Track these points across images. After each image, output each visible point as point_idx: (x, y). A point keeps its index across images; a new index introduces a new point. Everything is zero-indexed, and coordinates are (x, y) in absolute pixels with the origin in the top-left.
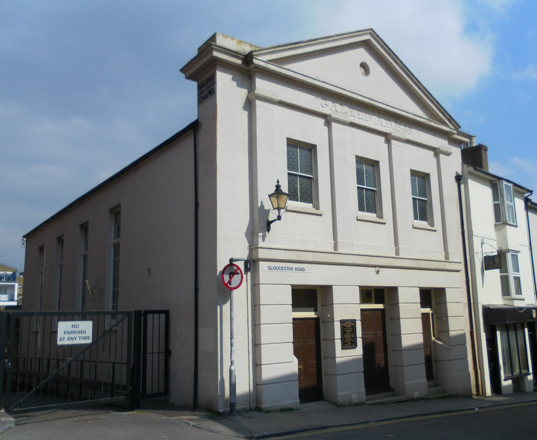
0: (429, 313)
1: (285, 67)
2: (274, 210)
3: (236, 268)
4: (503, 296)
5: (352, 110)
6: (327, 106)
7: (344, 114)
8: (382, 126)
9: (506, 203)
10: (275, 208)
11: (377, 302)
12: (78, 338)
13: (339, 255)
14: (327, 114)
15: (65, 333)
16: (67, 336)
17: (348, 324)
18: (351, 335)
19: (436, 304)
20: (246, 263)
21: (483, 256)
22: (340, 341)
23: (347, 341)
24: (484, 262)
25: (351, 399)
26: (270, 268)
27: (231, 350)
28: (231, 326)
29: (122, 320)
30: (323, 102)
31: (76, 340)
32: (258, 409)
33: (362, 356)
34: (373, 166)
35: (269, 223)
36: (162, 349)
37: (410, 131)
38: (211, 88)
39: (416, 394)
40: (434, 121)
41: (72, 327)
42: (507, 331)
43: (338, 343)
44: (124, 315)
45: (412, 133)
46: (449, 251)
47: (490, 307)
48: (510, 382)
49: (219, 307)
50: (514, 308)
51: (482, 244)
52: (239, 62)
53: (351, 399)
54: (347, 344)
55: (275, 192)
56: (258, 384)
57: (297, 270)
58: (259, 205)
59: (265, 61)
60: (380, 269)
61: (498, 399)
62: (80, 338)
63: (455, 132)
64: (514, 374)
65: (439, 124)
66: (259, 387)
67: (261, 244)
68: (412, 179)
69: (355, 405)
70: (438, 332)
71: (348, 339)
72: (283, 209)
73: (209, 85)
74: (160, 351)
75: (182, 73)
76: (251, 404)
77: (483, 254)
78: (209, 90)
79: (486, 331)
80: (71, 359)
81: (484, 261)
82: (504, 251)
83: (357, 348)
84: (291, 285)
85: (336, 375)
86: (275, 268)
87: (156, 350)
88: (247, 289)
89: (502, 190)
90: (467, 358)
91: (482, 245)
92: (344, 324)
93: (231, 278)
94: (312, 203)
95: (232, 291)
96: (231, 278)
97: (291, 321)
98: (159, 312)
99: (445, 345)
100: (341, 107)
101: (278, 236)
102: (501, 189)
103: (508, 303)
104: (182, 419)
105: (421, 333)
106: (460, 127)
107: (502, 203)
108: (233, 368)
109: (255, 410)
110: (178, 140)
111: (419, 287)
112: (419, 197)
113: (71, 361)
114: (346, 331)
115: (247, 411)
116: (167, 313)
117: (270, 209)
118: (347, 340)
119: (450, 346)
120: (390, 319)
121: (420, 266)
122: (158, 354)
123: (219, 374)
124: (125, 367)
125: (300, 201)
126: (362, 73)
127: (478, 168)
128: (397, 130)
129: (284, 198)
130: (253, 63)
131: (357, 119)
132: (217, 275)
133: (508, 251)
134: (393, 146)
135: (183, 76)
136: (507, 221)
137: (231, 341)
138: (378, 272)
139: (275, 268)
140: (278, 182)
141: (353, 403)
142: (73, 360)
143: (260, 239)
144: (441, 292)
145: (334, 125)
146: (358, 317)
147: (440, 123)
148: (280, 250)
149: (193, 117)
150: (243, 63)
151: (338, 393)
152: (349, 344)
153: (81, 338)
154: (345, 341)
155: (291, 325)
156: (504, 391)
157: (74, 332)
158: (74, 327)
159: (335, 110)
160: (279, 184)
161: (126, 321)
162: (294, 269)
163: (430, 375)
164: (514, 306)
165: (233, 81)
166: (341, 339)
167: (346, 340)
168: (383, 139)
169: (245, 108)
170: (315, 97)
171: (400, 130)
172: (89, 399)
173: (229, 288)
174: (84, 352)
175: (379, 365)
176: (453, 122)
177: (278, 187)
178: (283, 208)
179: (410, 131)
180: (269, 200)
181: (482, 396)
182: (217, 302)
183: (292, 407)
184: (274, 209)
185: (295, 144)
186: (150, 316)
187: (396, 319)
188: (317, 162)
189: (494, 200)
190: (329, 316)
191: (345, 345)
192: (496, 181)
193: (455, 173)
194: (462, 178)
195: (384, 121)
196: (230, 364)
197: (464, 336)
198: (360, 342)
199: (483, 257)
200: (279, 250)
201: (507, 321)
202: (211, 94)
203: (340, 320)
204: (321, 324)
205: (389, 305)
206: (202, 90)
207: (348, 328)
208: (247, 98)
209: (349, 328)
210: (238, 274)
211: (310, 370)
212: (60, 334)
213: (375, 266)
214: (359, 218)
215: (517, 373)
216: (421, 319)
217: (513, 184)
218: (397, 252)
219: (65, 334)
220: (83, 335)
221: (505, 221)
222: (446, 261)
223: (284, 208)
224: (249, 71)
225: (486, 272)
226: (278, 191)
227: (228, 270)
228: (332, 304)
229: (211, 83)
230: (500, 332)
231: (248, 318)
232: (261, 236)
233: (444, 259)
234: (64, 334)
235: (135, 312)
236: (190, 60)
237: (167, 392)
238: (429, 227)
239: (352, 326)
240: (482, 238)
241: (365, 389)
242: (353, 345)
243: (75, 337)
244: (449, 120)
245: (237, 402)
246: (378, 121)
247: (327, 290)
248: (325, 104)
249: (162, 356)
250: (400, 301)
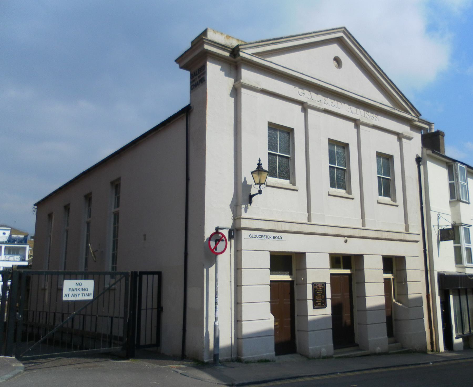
0: (391, 278)
1: (267, 59)
2: (255, 185)
3: (221, 236)
4: (456, 264)
5: (326, 98)
6: (304, 94)
7: (319, 102)
8: (352, 113)
9: (460, 183)
10: (256, 183)
11: (345, 268)
12: (81, 295)
13: (312, 225)
14: (304, 102)
15: (69, 290)
16: (71, 293)
17: (319, 287)
18: (321, 296)
19: (397, 270)
20: (230, 231)
21: (439, 228)
22: (312, 301)
23: (318, 301)
24: (440, 234)
25: (320, 352)
26: (251, 236)
27: (216, 308)
28: (216, 287)
29: (120, 280)
30: (301, 91)
31: (79, 296)
32: (239, 360)
33: (330, 315)
34: (344, 148)
35: (251, 197)
36: (155, 306)
37: (376, 117)
38: (202, 77)
39: (378, 349)
40: (398, 109)
41: (76, 285)
42: (459, 295)
43: (310, 303)
44: (122, 276)
45: (378, 119)
46: (409, 224)
47: (444, 274)
48: (460, 340)
49: (205, 270)
50: (466, 275)
51: (438, 218)
52: (227, 54)
53: (320, 352)
54: (318, 304)
55: (257, 169)
56: (239, 338)
57: (275, 238)
58: (243, 180)
59: (250, 53)
60: (348, 239)
61: (450, 354)
62: (83, 295)
63: (416, 119)
64: (465, 333)
65: (402, 112)
66: (240, 340)
67: (244, 215)
68: (377, 160)
69: (324, 358)
70: (398, 295)
71: (319, 300)
72: (264, 185)
73: (200, 74)
74: (153, 308)
75: (177, 63)
76: (232, 355)
77: (439, 227)
78: (200, 78)
79: (440, 294)
80: (74, 313)
81: (439, 233)
82: (458, 225)
83: (326, 308)
84: (269, 251)
85: (308, 331)
86: (256, 236)
87: (149, 306)
88: (231, 254)
89: (456, 171)
90: (423, 318)
91: (438, 219)
92: (316, 287)
93: (216, 244)
94: (289, 180)
95: (217, 256)
96: (216, 244)
97: (269, 283)
98: (153, 273)
99: (404, 306)
100: (316, 95)
101: (259, 208)
102: (456, 170)
103: (461, 270)
104: (171, 367)
105: (383, 295)
106: (420, 115)
107: (457, 182)
108: (217, 323)
109: (236, 361)
110: (172, 122)
111: (382, 255)
112: (383, 176)
113: (74, 315)
114: (317, 293)
115: (229, 361)
116: (159, 274)
117: (252, 184)
118: (318, 301)
119: (408, 307)
120: (356, 283)
121: (383, 237)
122: (151, 310)
123: (205, 329)
124: (122, 321)
125: (279, 178)
126: (335, 66)
127: (436, 151)
128: (365, 117)
129: (265, 174)
131: (330, 106)
132: (204, 241)
133: (461, 225)
134: (361, 131)
135: (178, 65)
136: (460, 199)
137: (216, 300)
138: (346, 241)
139: (256, 236)
140: (259, 160)
141: (323, 356)
142: (76, 314)
143: (243, 210)
144: (401, 259)
145: (310, 111)
146: (327, 280)
148: (261, 221)
149: (185, 102)
150: (230, 55)
151: (309, 347)
152: (319, 304)
153: (84, 295)
154: (316, 301)
155: (269, 287)
156: (455, 348)
157: (77, 290)
158: (78, 285)
159: (311, 98)
160: (261, 162)
161: (123, 280)
162: (272, 237)
163: (390, 333)
164: (465, 273)
165: (221, 71)
166: (313, 300)
167: (317, 301)
168: (352, 124)
169: (231, 95)
170: (293, 86)
171: (368, 117)
172: (90, 349)
173: (215, 253)
174: (86, 307)
175: (346, 323)
176: (414, 110)
177: (259, 165)
178: (263, 184)
180: (252, 175)
181: (436, 352)
182: (204, 266)
183: (268, 358)
184: (256, 184)
185: (275, 128)
186: (144, 277)
187: (362, 283)
188: (294, 143)
189: (450, 180)
190: (302, 279)
191: (316, 305)
192: (452, 163)
193: (416, 155)
194: (422, 159)
195: (353, 109)
196: (215, 320)
197: (420, 299)
198: (329, 302)
199: (439, 230)
200: (260, 221)
201: (459, 287)
202: (202, 82)
203: (312, 283)
204: (295, 287)
205: (356, 270)
206: (194, 79)
207: (319, 290)
208: (234, 86)
209: (320, 290)
210: (223, 241)
211: (285, 326)
212: (65, 291)
213: (344, 236)
214: (330, 194)
215: (467, 332)
216: (383, 284)
217: (466, 166)
218: (363, 224)
219: (70, 291)
220: (85, 292)
221: (459, 198)
222: (406, 232)
223: (264, 184)
224: (236, 62)
225: (441, 243)
226: (259, 169)
227: (214, 238)
228: (305, 269)
229: (202, 73)
230: (453, 296)
231: (231, 280)
232: (244, 208)
233: (404, 231)
234: (69, 291)
235: (132, 272)
236: (184, 52)
237: (158, 343)
238: (392, 203)
239: (322, 288)
240: (438, 213)
241: (333, 344)
242: (323, 305)
243: (78, 294)
244: (411, 109)
245: (220, 353)
246: (349, 109)
247: (301, 256)
248: (302, 93)
249: (155, 312)
250: (365, 267)
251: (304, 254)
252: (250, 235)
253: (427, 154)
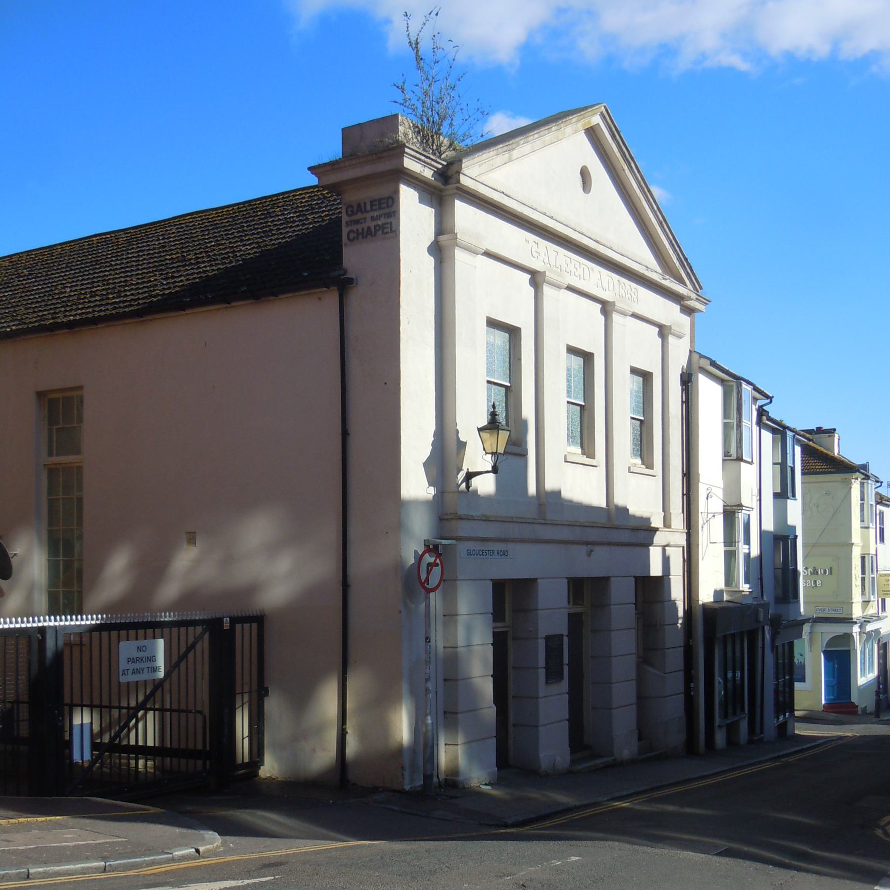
10: (487, 452)
12: (146, 670)
15: (128, 661)
29: (202, 634)
46: (671, 511)
62: (148, 670)
75: (312, 173)
83: (562, 681)
106: (701, 288)
138: (589, 554)
147: (677, 281)
157: (140, 660)
161: (207, 636)
162: (496, 553)
166: (545, 668)
173: (425, 588)
179: (635, 295)
184: (486, 453)
186: (238, 627)
204: (510, 643)
206: (355, 217)
213: (587, 543)
224: (441, 191)
229: (386, 211)
240: (708, 486)
246: (598, 280)
248: (536, 252)
251: (534, 581)
252: (468, 550)
253: (700, 366)
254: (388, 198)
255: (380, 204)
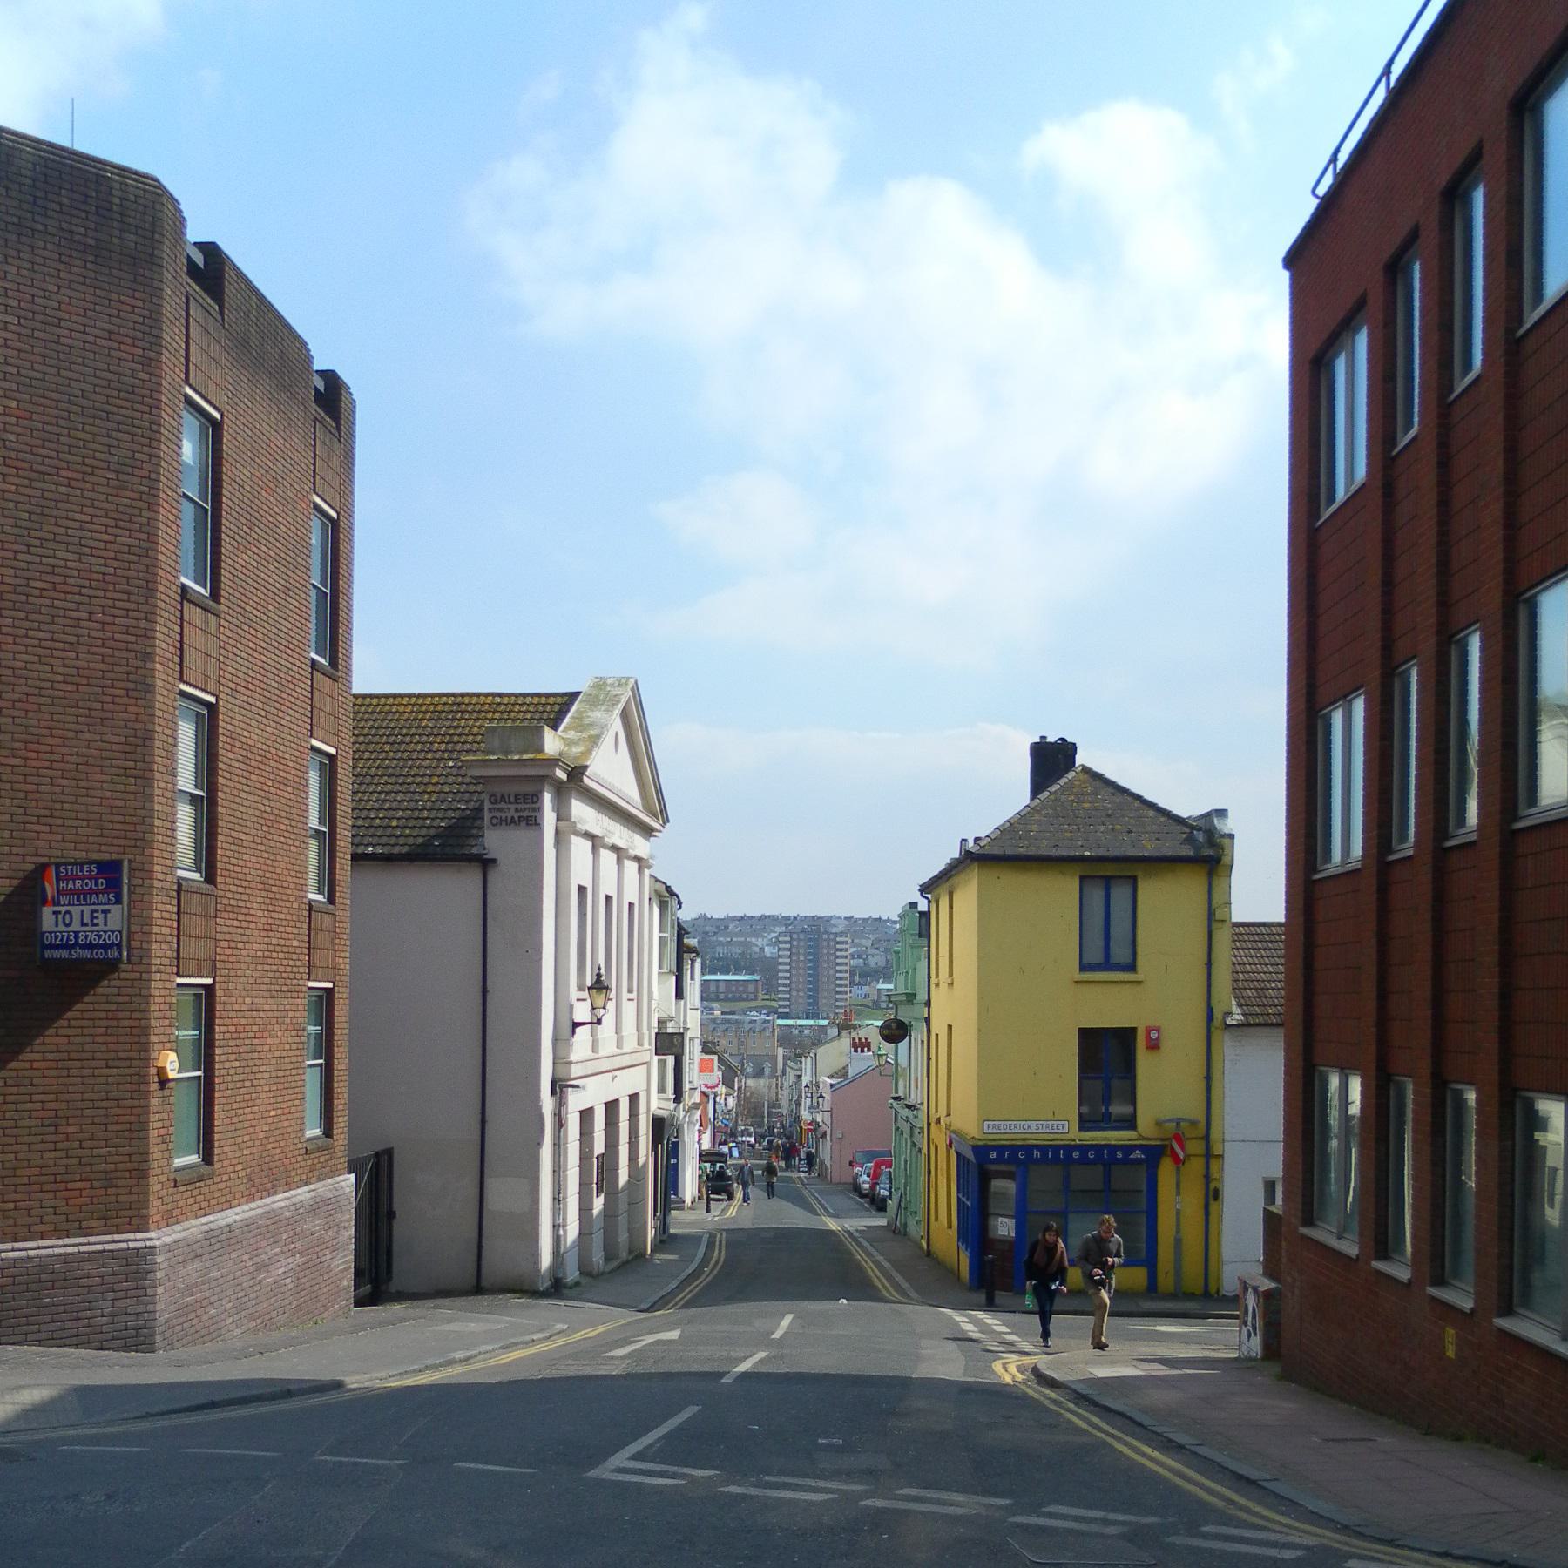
73: (522, 806)
78: (525, 814)
130: (582, 781)
254: (533, 796)
255: (525, 799)
